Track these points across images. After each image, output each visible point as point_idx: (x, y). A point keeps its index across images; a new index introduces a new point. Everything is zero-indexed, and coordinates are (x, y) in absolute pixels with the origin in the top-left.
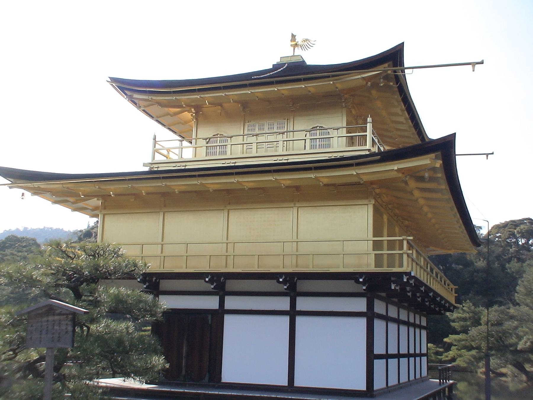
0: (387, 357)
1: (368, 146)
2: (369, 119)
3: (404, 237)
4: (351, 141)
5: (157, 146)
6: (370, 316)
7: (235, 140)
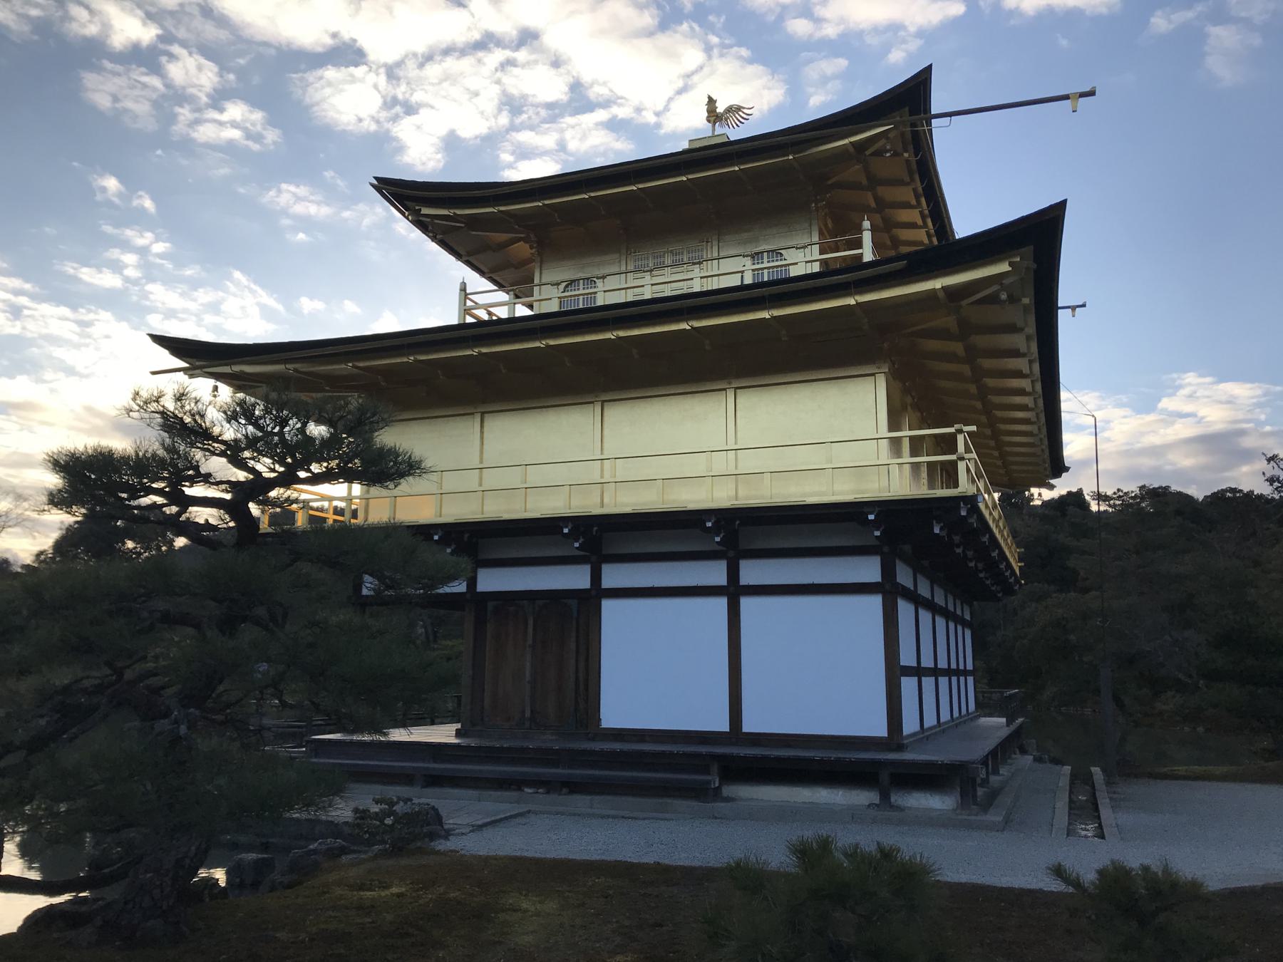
0: (918, 672)
2: (867, 224)
3: (957, 426)
5: (469, 303)
6: (888, 590)
7: (612, 282)
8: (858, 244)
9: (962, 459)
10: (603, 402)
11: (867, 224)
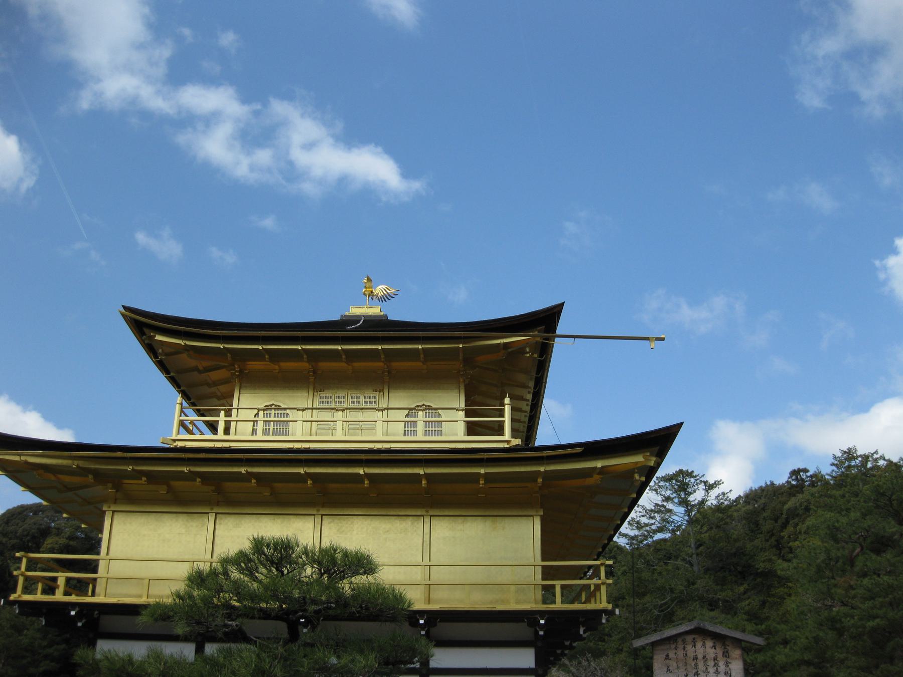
1: (507, 435)
2: (507, 400)
4: (472, 429)
9: (603, 584)
10: (322, 515)
11: (507, 400)
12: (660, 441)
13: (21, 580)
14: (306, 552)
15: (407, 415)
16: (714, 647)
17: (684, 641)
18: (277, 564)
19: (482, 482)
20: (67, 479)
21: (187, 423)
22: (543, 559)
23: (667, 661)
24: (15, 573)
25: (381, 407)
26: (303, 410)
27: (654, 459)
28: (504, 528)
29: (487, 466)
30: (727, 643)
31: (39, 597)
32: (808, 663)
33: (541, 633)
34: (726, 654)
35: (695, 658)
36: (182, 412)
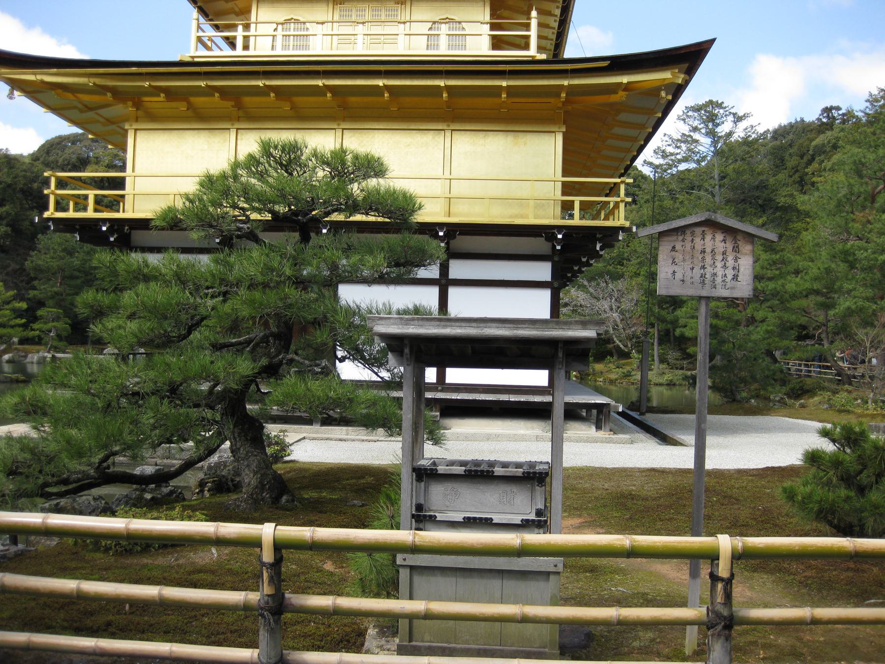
2: (534, 13)
4: (497, 43)
8: (527, 27)
9: (622, 201)
10: (343, 129)
11: (534, 13)
12: (689, 58)
13: (52, 199)
14: (315, 154)
15: (430, 29)
16: (724, 241)
17: (693, 234)
18: (285, 166)
19: (504, 96)
20: (86, 98)
21: (205, 40)
22: (563, 176)
23: (673, 253)
24: (46, 192)
25: (403, 20)
26: (323, 23)
27: (682, 76)
28: (525, 144)
29: (509, 79)
30: (738, 237)
31: (71, 214)
32: (817, 292)
33: (558, 248)
34: (736, 249)
35: (703, 252)
36: (199, 28)
